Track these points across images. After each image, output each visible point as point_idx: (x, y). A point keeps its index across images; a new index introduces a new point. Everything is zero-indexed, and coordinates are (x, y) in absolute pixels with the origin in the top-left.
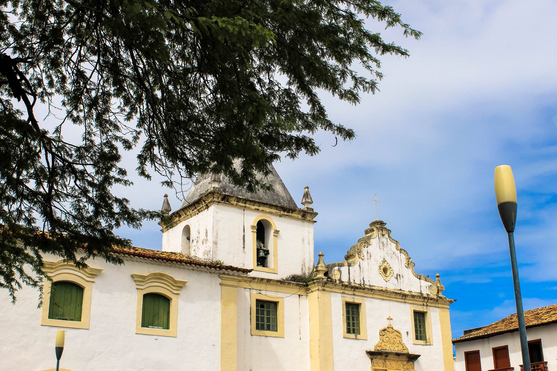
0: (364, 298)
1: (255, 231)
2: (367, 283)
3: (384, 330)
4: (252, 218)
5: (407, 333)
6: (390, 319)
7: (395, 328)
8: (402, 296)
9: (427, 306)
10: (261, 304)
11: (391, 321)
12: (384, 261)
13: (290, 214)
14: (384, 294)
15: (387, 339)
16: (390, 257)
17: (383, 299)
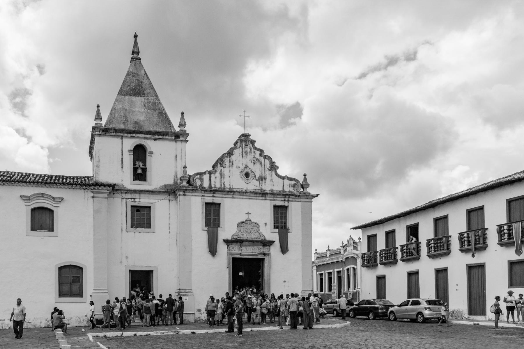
0: (224, 199)
1: (132, 153)
2: (227, 186)
3: (242, 223)
4: (130, 143)
5: (266, 224)
6: (248, 214)
7: (253, 221)
8: (263, 194)
9: (288, 201)
10: (136, 209)
12: (246, 167)
14: (244, 193)
15: (245, 229)
17: (243, 198)
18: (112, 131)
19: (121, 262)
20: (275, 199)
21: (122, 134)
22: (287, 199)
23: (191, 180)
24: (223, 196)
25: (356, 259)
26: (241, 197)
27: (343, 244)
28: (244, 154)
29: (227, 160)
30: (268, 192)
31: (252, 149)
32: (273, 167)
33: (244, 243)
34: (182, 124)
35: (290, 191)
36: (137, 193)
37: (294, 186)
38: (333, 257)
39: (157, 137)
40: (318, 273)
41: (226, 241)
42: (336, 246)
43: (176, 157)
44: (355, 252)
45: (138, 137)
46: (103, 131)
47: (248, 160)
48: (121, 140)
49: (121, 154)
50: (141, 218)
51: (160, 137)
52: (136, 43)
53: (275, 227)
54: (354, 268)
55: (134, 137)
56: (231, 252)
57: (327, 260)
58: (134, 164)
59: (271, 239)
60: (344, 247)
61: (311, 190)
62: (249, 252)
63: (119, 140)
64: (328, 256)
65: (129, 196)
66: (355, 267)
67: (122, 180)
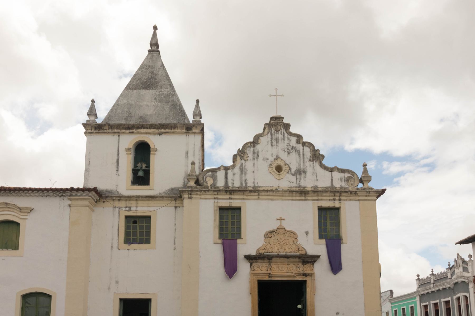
2: (250, 184)
3: (272, 232)
5: (307, 233)
6: (281, 219)
7: (287, 229)
8: (302, 193)
9: (340, 200)
11: (283, 221)
12: (277, 158)
13: (173, 130)
15: (276, 241)
16: (286, 153)
17: (272, 200)
18: (107, 127)
19: (109, 288)
20: (320, 198)
21: (119, 131)
22: (337, 198)
23: (200, 179)
24: (245, 197)
25: (468, 285)
26: (270, 197)
27: (449, 265)
28: (275, 142)
29: (250, 152)
30: (309, 189)
31: (286, 135)
32: (317, 156)
33: (274, 259)
34: (197, 114)
35: (342, 187)
36: (133, 200)
37: (347, 180)
38: (439, 284)
39: (162, 130)
40: (422, 304)
41: (248, 258)
42: (440, 269)
43: (187, 153)
44: (466, 274)
45: (138, 133)
46: (96, 128)
47: (280, 150)
48: (117, 138)
49: (117, 153)
50: (137, 230)
51: (167, 130)
52: (155, 35)
53: (321, 237)
54: (466, 297)
55: (133, 132)
56: (256, 272)
57: (432, 288)
58: (136, 165)
59: (315, 253)
60: (451, 269)
61: (374, 185)
62: (282, 272)
63: (115, 138)
64: (432, 282)
65: (123, 204)
66: (467, 295)
67: (117, 186)
